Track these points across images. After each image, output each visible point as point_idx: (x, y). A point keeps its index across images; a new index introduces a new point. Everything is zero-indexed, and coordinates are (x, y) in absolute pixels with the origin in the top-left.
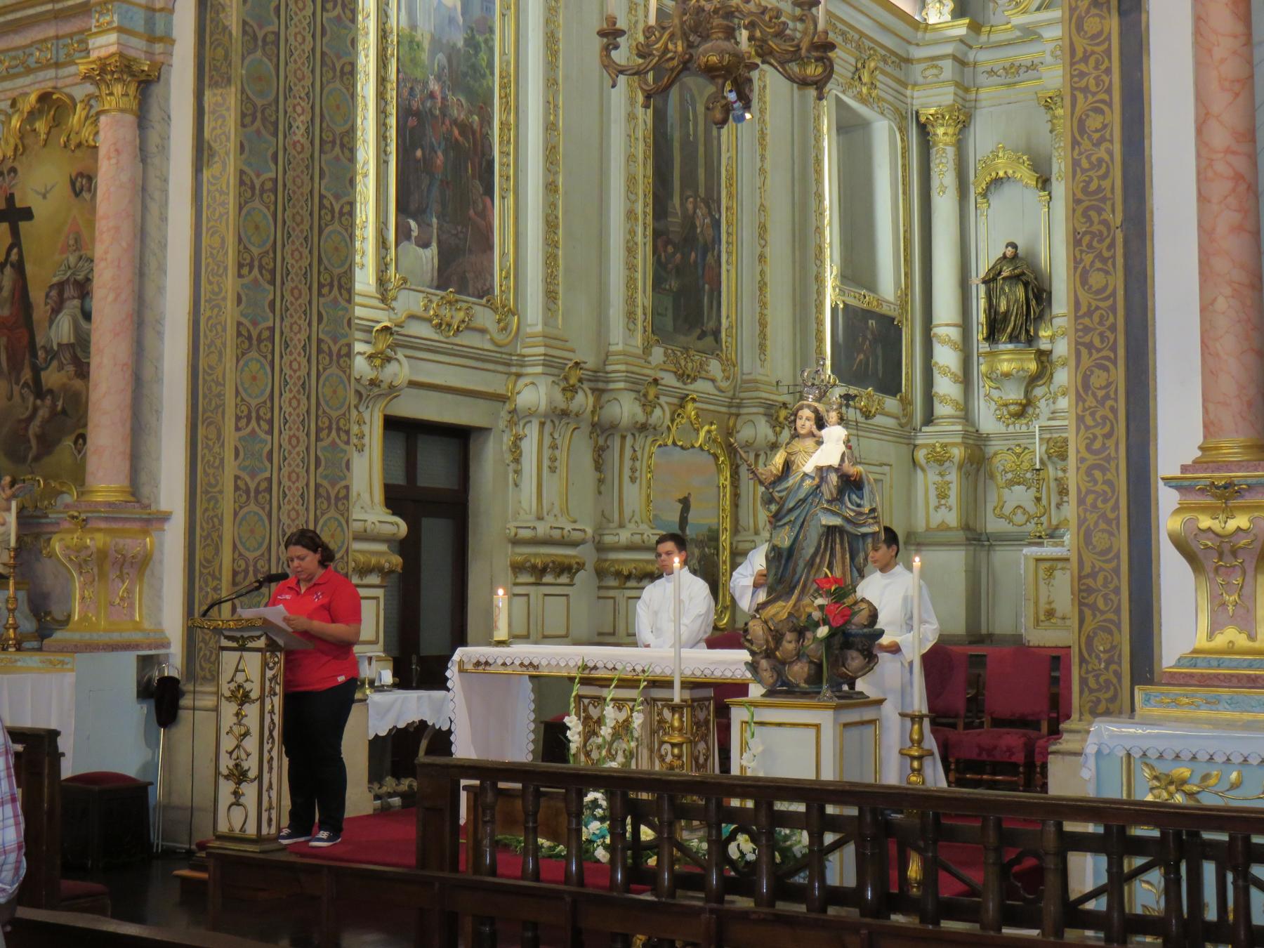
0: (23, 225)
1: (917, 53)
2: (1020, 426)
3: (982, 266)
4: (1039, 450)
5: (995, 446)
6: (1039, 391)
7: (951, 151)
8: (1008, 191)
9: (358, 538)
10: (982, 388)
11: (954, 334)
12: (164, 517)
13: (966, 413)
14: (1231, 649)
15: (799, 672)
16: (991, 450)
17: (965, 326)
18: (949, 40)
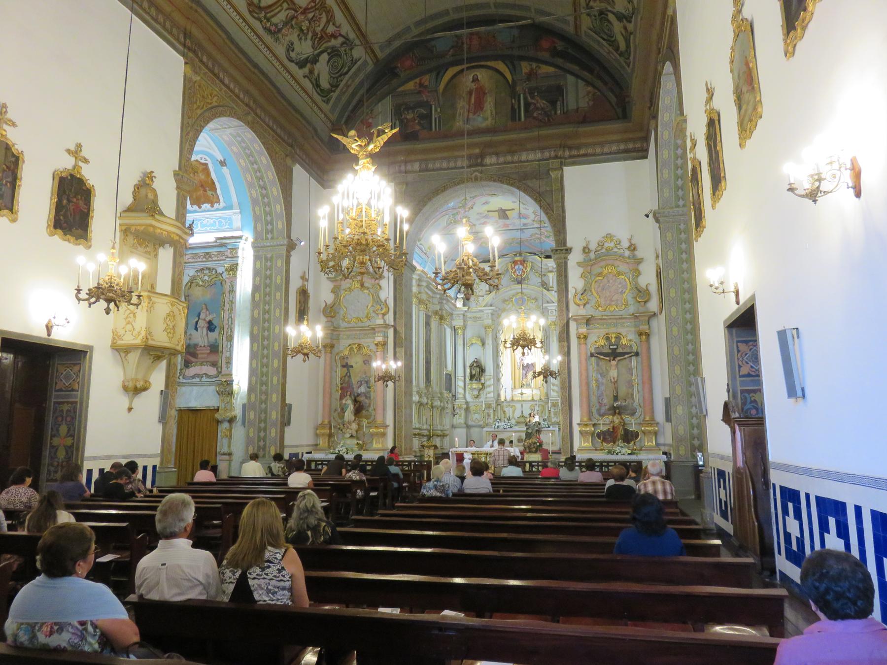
0: (351, 369)
1: (454, 313)
2: (476, 400)
3: (468, 364)
4: (484, 406)
5: (470, 405)
6: (481, 392)
7: (462, 336)
8: (474, 346)
9: (414, 429)
10: (467, 392)
11: (463, 378)
12: (388, 426)
13: (465, 398)
14: (587, 446)
15: (534, 449)
16: (470, 405)
17: (465, 377)
18: (462, 311)
